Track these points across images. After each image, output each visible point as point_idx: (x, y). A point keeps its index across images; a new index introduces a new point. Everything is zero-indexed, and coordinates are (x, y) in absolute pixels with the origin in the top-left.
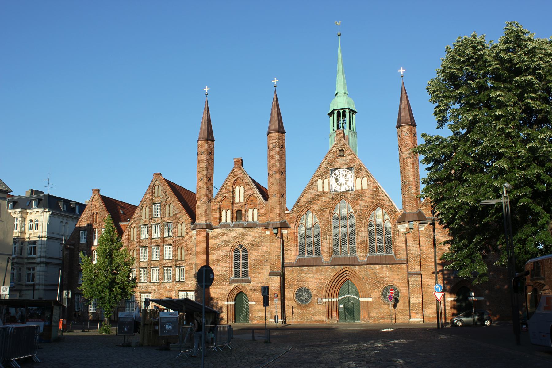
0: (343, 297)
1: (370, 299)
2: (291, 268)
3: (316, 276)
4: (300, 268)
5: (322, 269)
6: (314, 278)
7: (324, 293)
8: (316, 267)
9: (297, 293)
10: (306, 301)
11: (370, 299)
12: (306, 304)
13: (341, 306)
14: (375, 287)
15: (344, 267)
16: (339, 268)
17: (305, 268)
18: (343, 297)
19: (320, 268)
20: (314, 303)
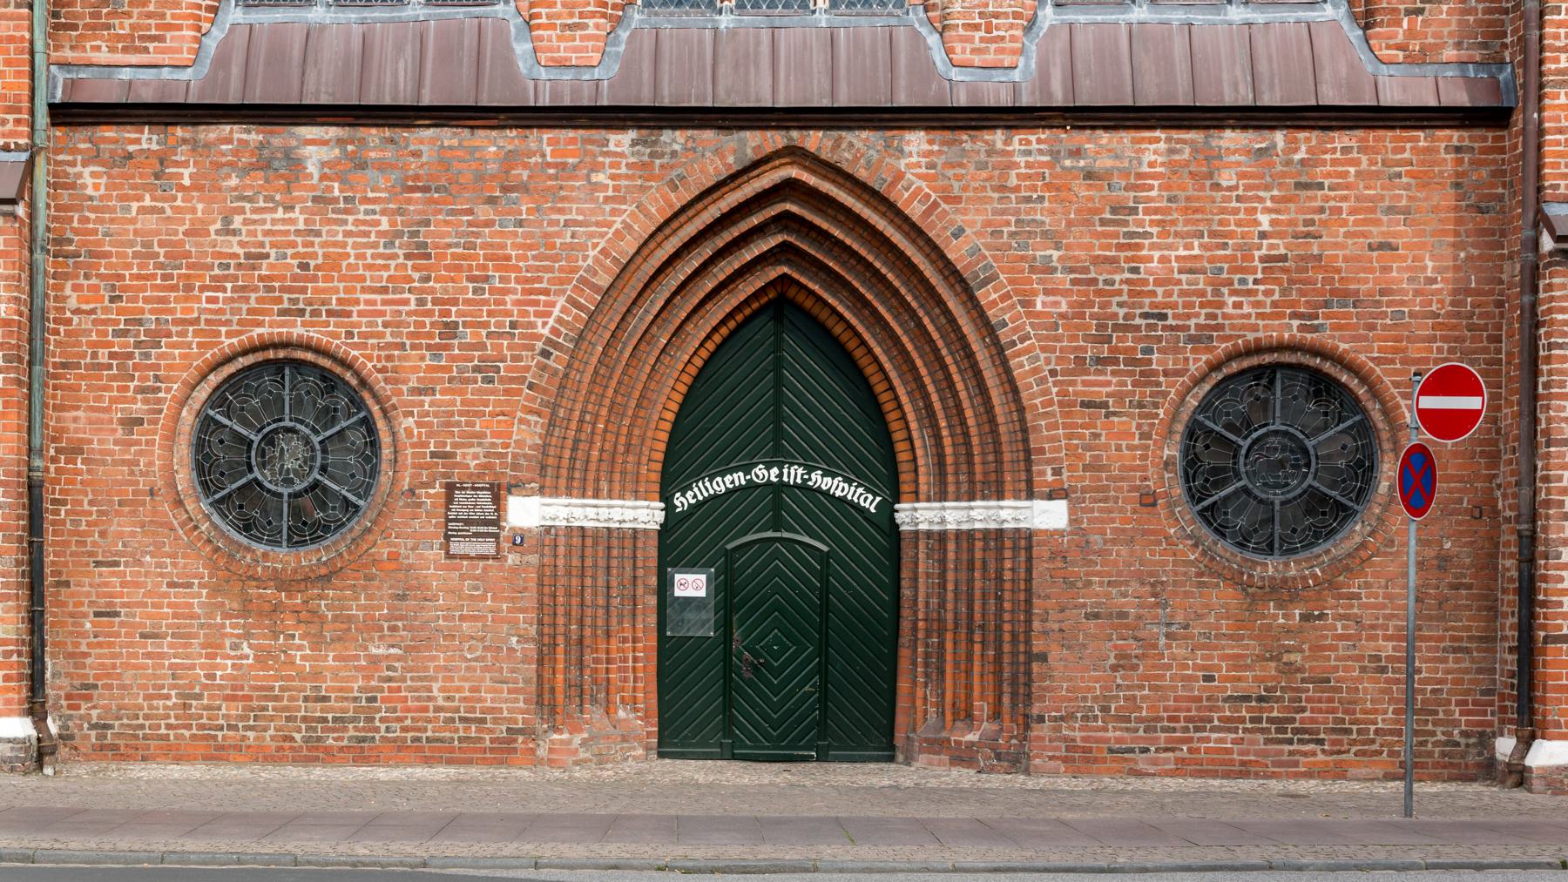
0: (721, 485)
1: (1049, 516)
2: (146, 139)
3: (444, 233)
4: (253, 135)
5: (510, 160)
6: (420, 253)
7: (527, 433)
8: (448, 137)
9: (206, 425)
10: (314, 516)
11: (1049, 516)
12: (310, 557)
13: (691, 585)
14: (1106, 385)
15: (775, 139)
16: (716, 153)
17: (316, 147)
18: (721, 485)
19: (493, 144)
20: (408, 535)
